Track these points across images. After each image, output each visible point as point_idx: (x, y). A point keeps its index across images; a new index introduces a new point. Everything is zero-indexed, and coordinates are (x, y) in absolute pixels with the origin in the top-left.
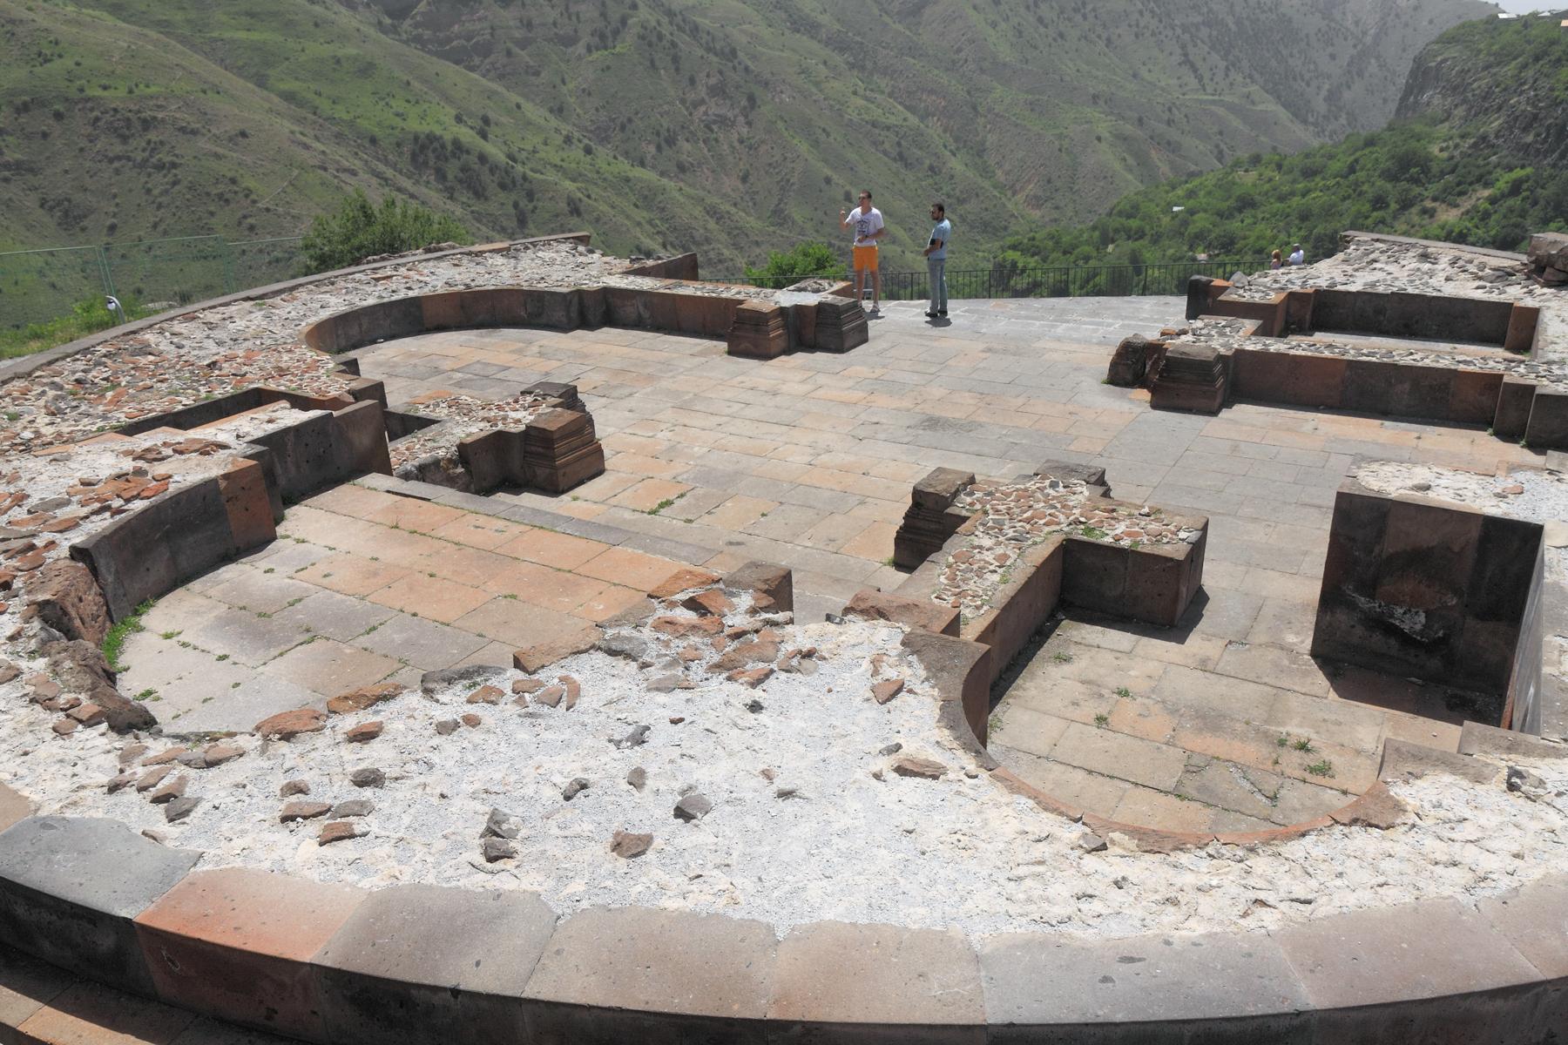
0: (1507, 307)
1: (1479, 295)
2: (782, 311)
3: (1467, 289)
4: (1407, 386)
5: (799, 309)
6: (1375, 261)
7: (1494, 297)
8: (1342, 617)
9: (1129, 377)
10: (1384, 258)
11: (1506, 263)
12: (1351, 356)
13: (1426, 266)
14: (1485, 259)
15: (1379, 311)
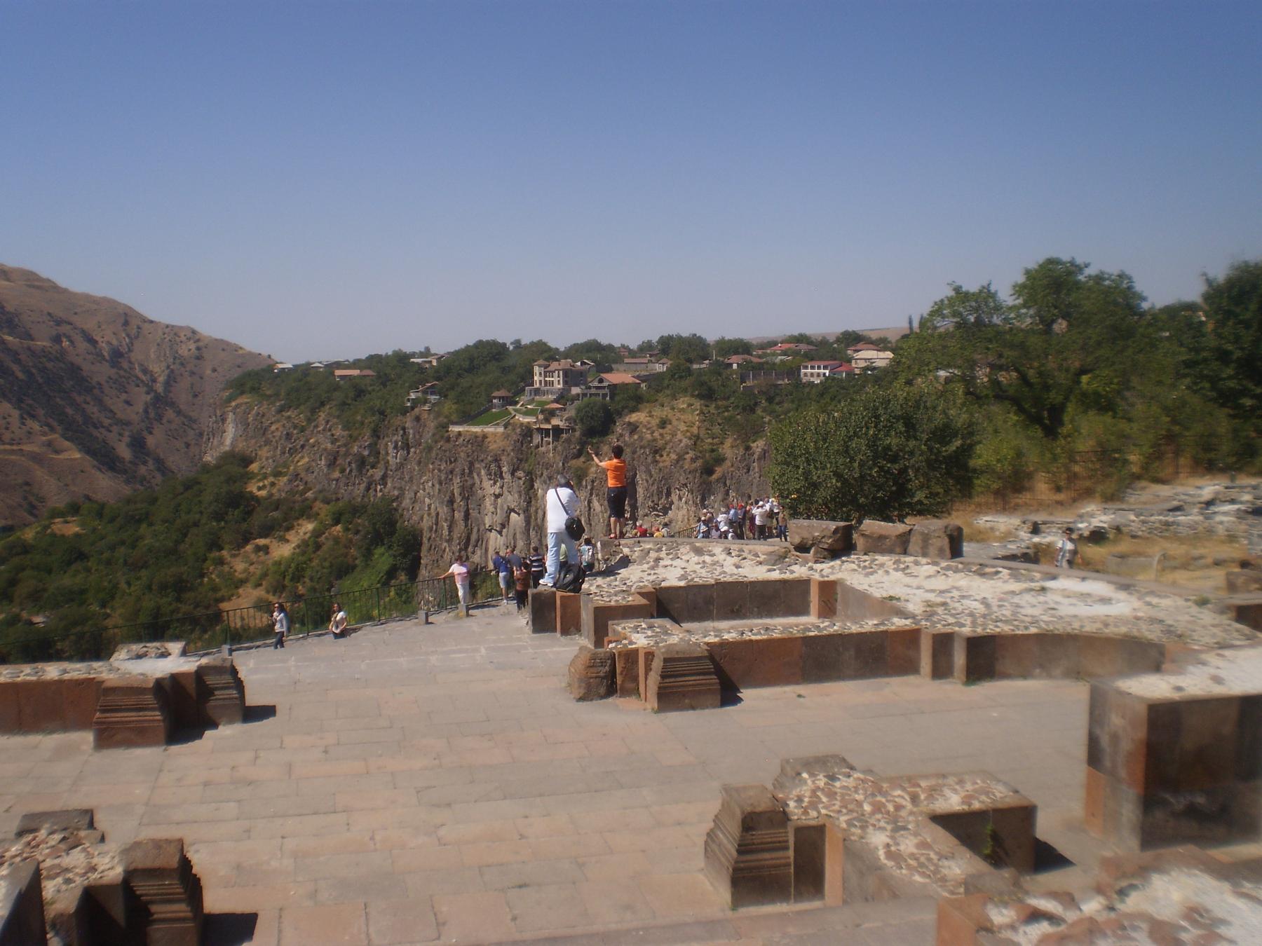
0: (804, 584)
1: (776, 575)
2: (159, 683)
3: (755, 572)
4: (852, 652)
5: (175, 678)
6: (658, 559)
7: (787, 576)
8: (1159, 815)
9: (602, 690)
10: (663, 554)
11: (771, 549)
12: (795, 632)
13: (707, 559)
14: (751, 547)
15: (709, 601)
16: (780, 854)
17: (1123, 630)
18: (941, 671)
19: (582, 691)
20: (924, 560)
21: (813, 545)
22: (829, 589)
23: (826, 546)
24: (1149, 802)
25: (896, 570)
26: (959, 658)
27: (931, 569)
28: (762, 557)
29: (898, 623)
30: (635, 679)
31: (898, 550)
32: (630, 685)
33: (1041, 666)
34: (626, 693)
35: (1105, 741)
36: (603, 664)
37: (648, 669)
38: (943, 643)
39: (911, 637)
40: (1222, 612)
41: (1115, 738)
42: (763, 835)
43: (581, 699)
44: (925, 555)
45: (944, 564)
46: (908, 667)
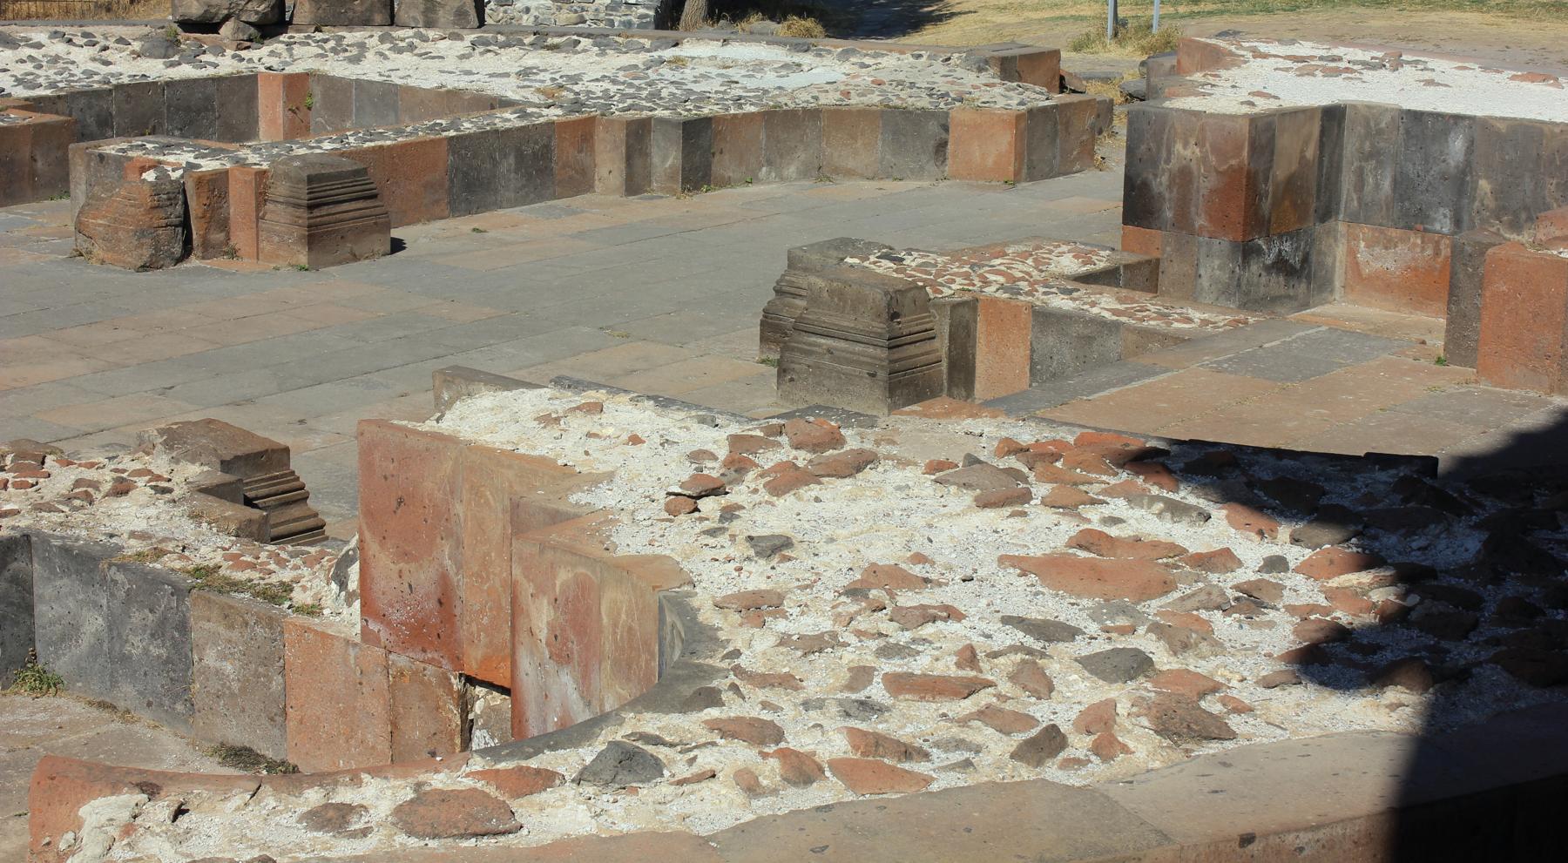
0: (245, 85)
4: (512, 160)
9: (177, 249)
16: (927, 346)
17: (875, 98)
18: (634, 184)
19: (146, 253)
20: (431, 33)
21: (227, 18)
22: (296, 85)
23: (254, 18)
24: (1247, 252)
25: (400, 51)
26: (666, 157)
27: (461, 47)
28: (136, 46)
29: (508, 119)
30: (224, 225)
31: (378, 18)
32: (217, 237)
33: (770, 163)
34: (209, 250)
35: (1161, 183)
36: (172, 200)
37: (262, 198)
38: (638, 133)
39: (582, 130)
40: (980, 70)
41: (1184, 176)
42: (907, 324)
43: (145, 268)
44: (429, 24)
45: (473, 37)
46: (581, 182)
